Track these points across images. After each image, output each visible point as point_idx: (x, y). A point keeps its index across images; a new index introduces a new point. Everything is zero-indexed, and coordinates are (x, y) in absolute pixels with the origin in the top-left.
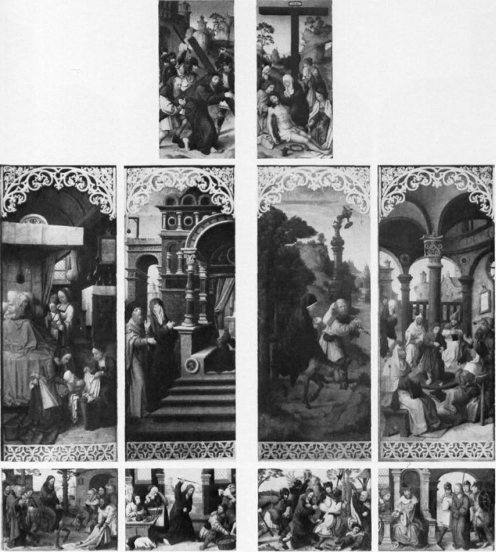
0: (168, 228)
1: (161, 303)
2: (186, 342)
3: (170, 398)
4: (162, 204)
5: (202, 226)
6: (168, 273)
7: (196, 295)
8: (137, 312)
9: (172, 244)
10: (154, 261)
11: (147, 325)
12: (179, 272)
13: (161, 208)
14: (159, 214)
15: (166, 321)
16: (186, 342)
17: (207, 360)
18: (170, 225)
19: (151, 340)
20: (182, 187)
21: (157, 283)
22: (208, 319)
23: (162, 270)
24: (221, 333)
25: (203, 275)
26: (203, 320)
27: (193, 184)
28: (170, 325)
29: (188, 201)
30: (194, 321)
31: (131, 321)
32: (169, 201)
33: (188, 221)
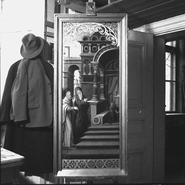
0: (84, 52)
1: (80, 89)
2: (93, 109)
3: (85, 137)
4: (81, 40)
5: (101, 51)
6: (84, 74)
7: (98, 85)
8: (68, 94)
9: (86, 59)
10: (77, 68)
11: (74, 101)
12: (90, 74)
13: (81, 42)
14: (80, 45)
15: (83, 98)
16: (93, 109)
17: (104, 117)
18: (85, 50)
19: (76, 108)
20: (91, 33)
21: (79, 79)
22: (105, 97)
23: (81, 73)
24: (112, 104)
25: (102, 75)
26: (102, 98)
27: (97, 30)
28: (85, 100)
29: (94, 39)
30: (98, 98)
31: (66, 98)
32: (85, 38)
33: (94, 48)
